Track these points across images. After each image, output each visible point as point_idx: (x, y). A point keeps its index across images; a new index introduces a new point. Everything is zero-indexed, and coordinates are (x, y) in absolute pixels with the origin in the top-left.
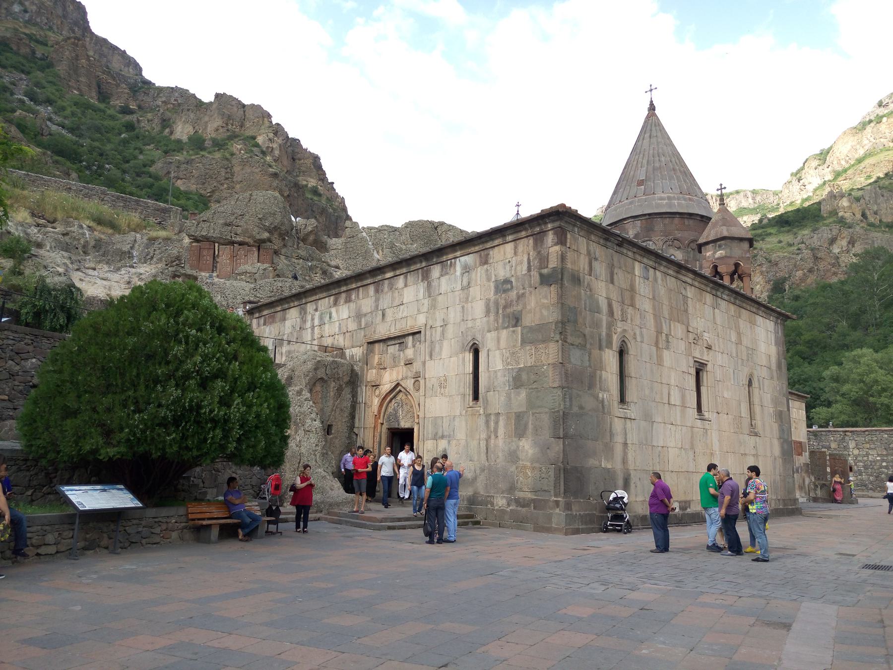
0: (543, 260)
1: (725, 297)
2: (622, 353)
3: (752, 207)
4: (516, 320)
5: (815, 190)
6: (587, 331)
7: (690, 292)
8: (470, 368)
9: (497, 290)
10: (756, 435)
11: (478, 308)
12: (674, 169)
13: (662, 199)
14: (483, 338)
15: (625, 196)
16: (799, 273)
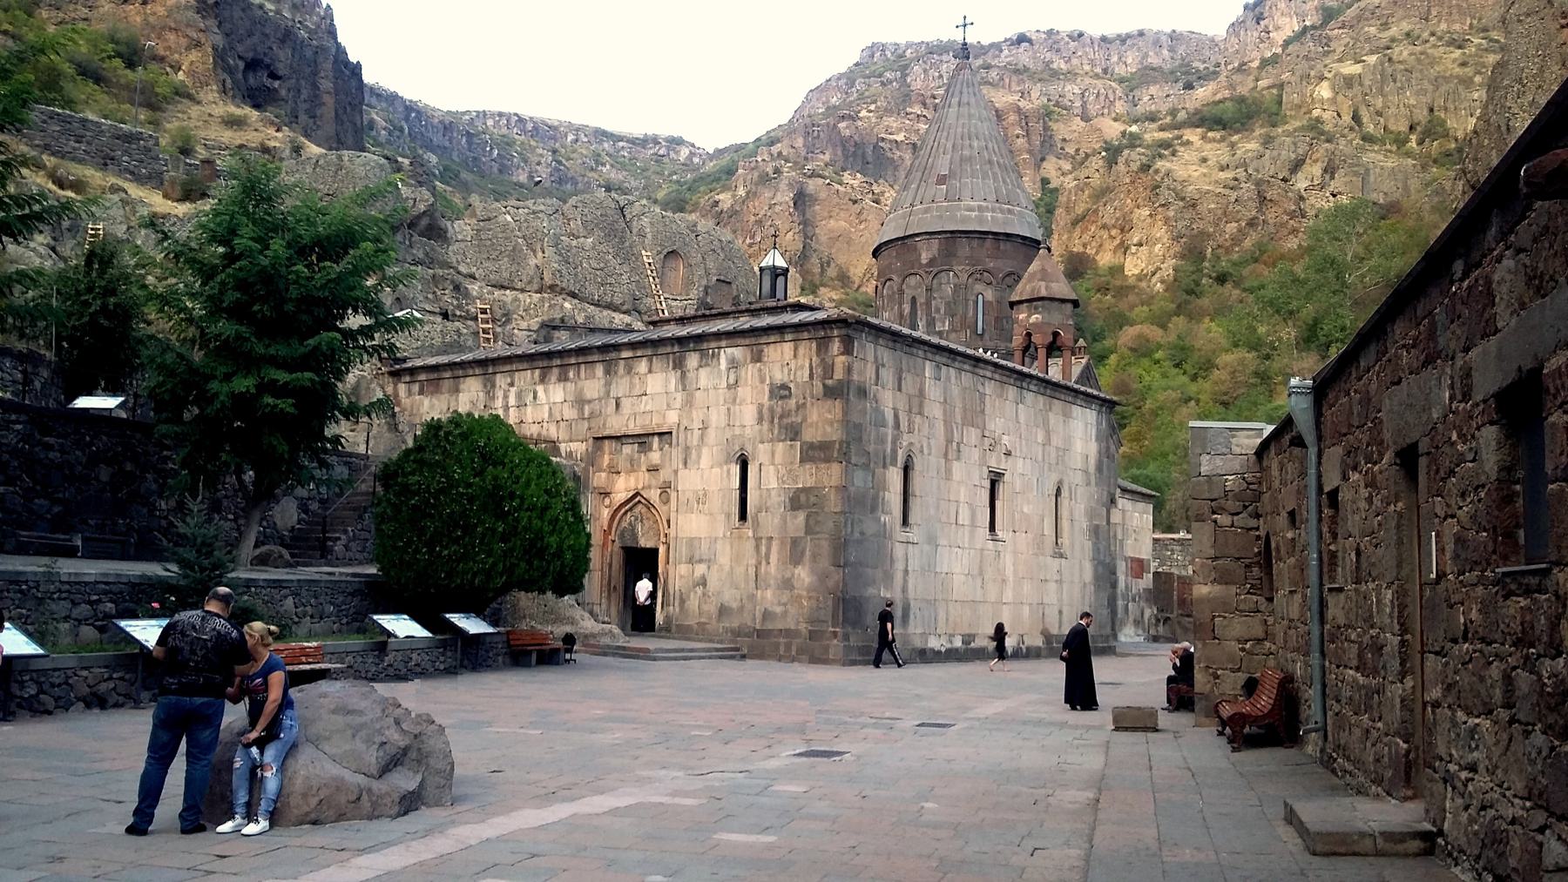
0: (828, 370)
1: (1032, 387)
2: (907, 470)
3: (1167, 67)
4: (793, 433)
5: (1287, 43)
6: (871, 448)
7: (989, 388)
8: (736, 483)
9: (772, 394)
10: (1061, 556)
11: (748, 414)
12: (990, 162)
13: (971, 209)
14: (755, 448)
15: (919, 198)
16: (1232, 227)
